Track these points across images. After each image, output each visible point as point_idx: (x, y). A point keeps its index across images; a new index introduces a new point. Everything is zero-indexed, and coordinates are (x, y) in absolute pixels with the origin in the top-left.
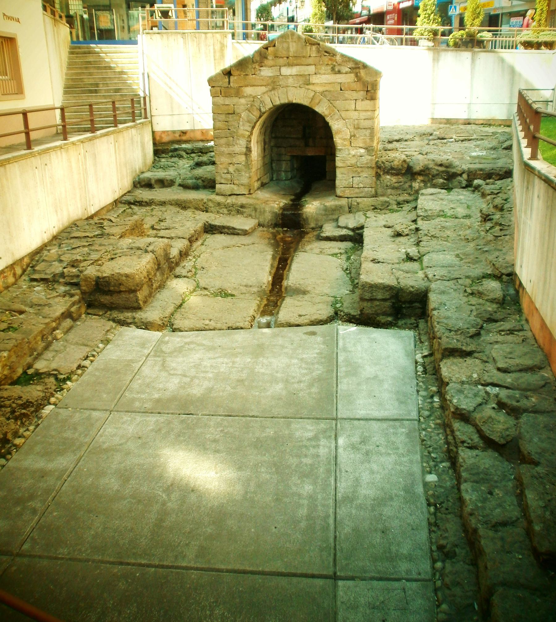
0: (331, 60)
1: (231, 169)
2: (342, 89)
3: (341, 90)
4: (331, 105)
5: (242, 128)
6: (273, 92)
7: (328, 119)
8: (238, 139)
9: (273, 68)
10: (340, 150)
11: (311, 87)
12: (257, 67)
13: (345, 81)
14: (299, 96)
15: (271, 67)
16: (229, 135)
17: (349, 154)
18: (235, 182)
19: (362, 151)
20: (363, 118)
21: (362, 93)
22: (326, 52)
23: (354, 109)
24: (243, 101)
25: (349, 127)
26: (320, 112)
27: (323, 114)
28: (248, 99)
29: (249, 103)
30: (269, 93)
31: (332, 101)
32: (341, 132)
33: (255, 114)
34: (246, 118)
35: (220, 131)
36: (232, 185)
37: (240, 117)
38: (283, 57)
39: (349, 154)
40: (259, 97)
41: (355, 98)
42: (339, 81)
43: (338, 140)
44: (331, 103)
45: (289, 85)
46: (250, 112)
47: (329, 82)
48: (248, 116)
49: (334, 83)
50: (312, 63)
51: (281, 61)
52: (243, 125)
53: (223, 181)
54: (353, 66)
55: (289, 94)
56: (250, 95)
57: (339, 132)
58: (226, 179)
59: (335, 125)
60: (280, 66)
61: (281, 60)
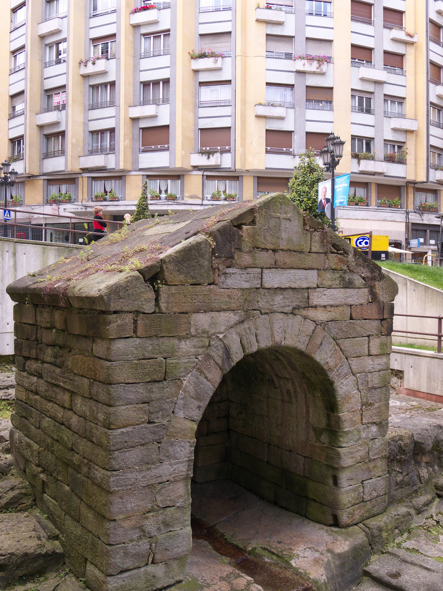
0: (341, 261)
1: (150, 525)
2: (354, 315)
3: (351, 318)
4: (337, 347)
5: (181, 414)
6: (246, 325)
7: (332, 375)
8: (172, 444)
9: (250, 270)
10: (347, 433)
11: (311, 313)
12: (221, 268)
13: (358, 302)
14: (287, 332)
15: (246, 268)
16: (151, 437)
17: (360, 438)
18: (158, 557)
19: (374, 429)
20: (379, 367)
21: (376, 324)
22: (334, 246)
23: (367, 353)
24: (186, 346)
25: (361, 387)
26: (322, 363)
27: (325, 367)
28: (195, 341)
29: (201, 350)
30: (240, 328)
31: (339, 342)
32: (350, 398)
33: (209, 376)
34: (191, 389)
35: (129, 429)
36: (151, 568)
37: (179, 387)
38: (267, 250)
39: (360, 438)
40: (221, 336)
41: (369, 333)
42: (350, 301)
43: (345, 414)
44: (338, 345)
45: (275, 308)
46: (202, 372)
47: (337, 303)
48: (197, 384)
49: (342, 306)
50: (314, 265)
51: (264, 258)
52: (185, 406)
53: (128, 564)
54: (369, 274)
55: (277, 327)
56: (204, 332)
57: (347, 398)
58: (137, 556)
59: (345, 387)
60: (262, 268)
61: (264, 255)
